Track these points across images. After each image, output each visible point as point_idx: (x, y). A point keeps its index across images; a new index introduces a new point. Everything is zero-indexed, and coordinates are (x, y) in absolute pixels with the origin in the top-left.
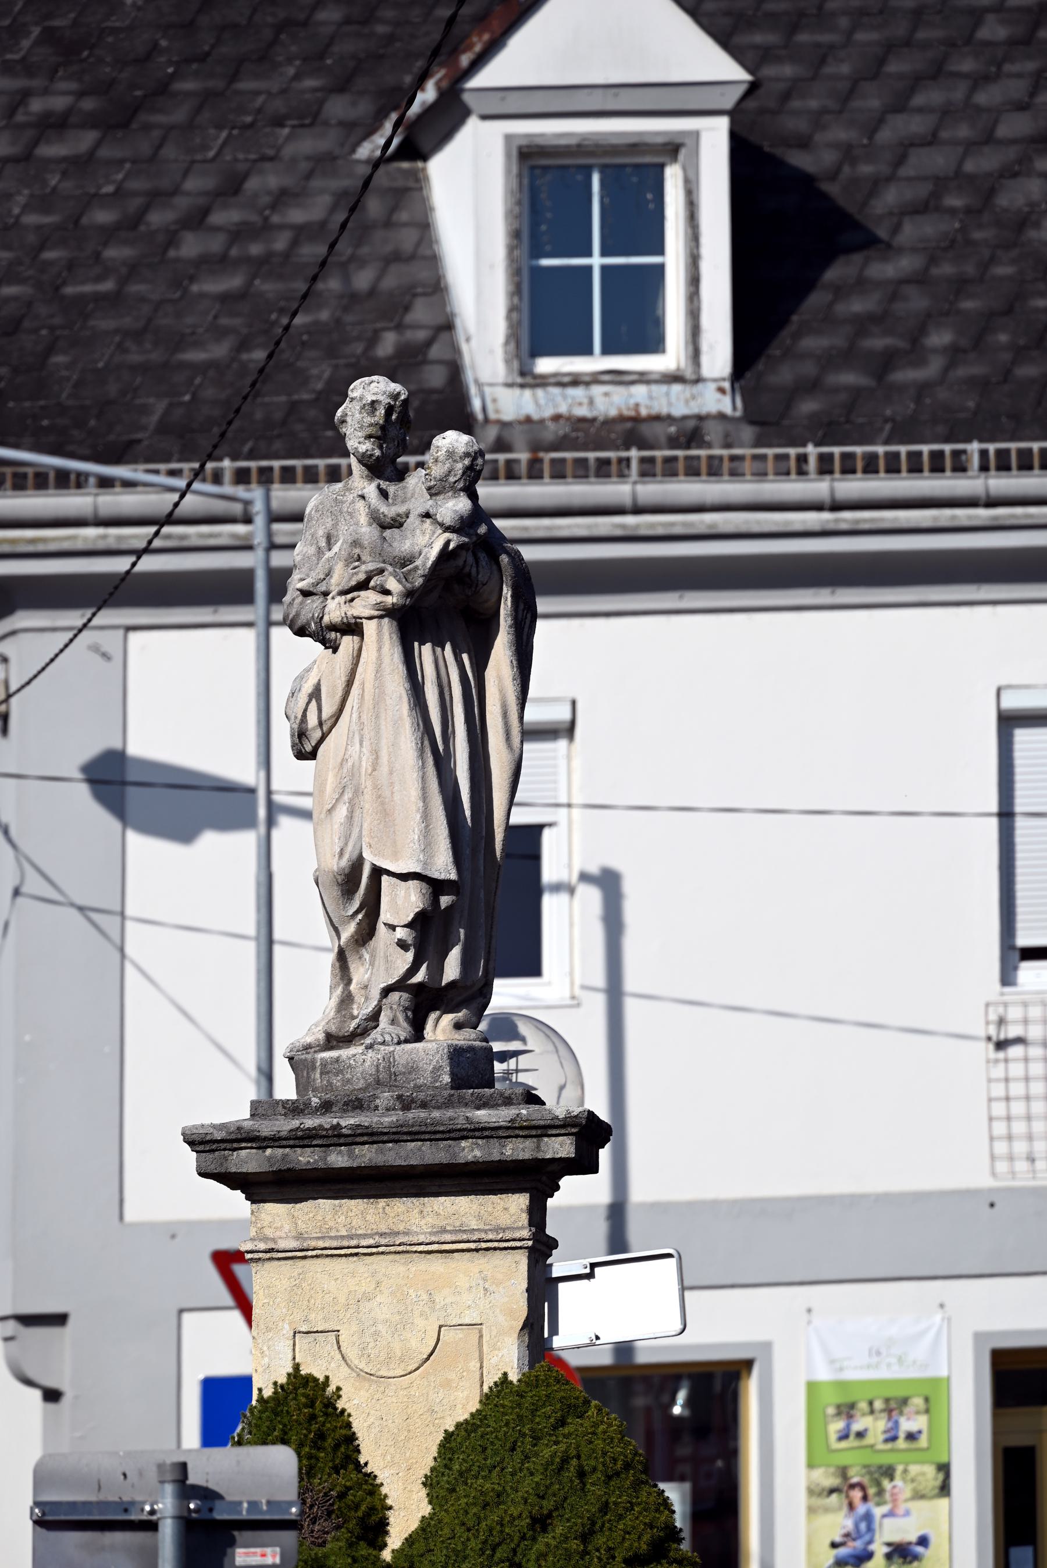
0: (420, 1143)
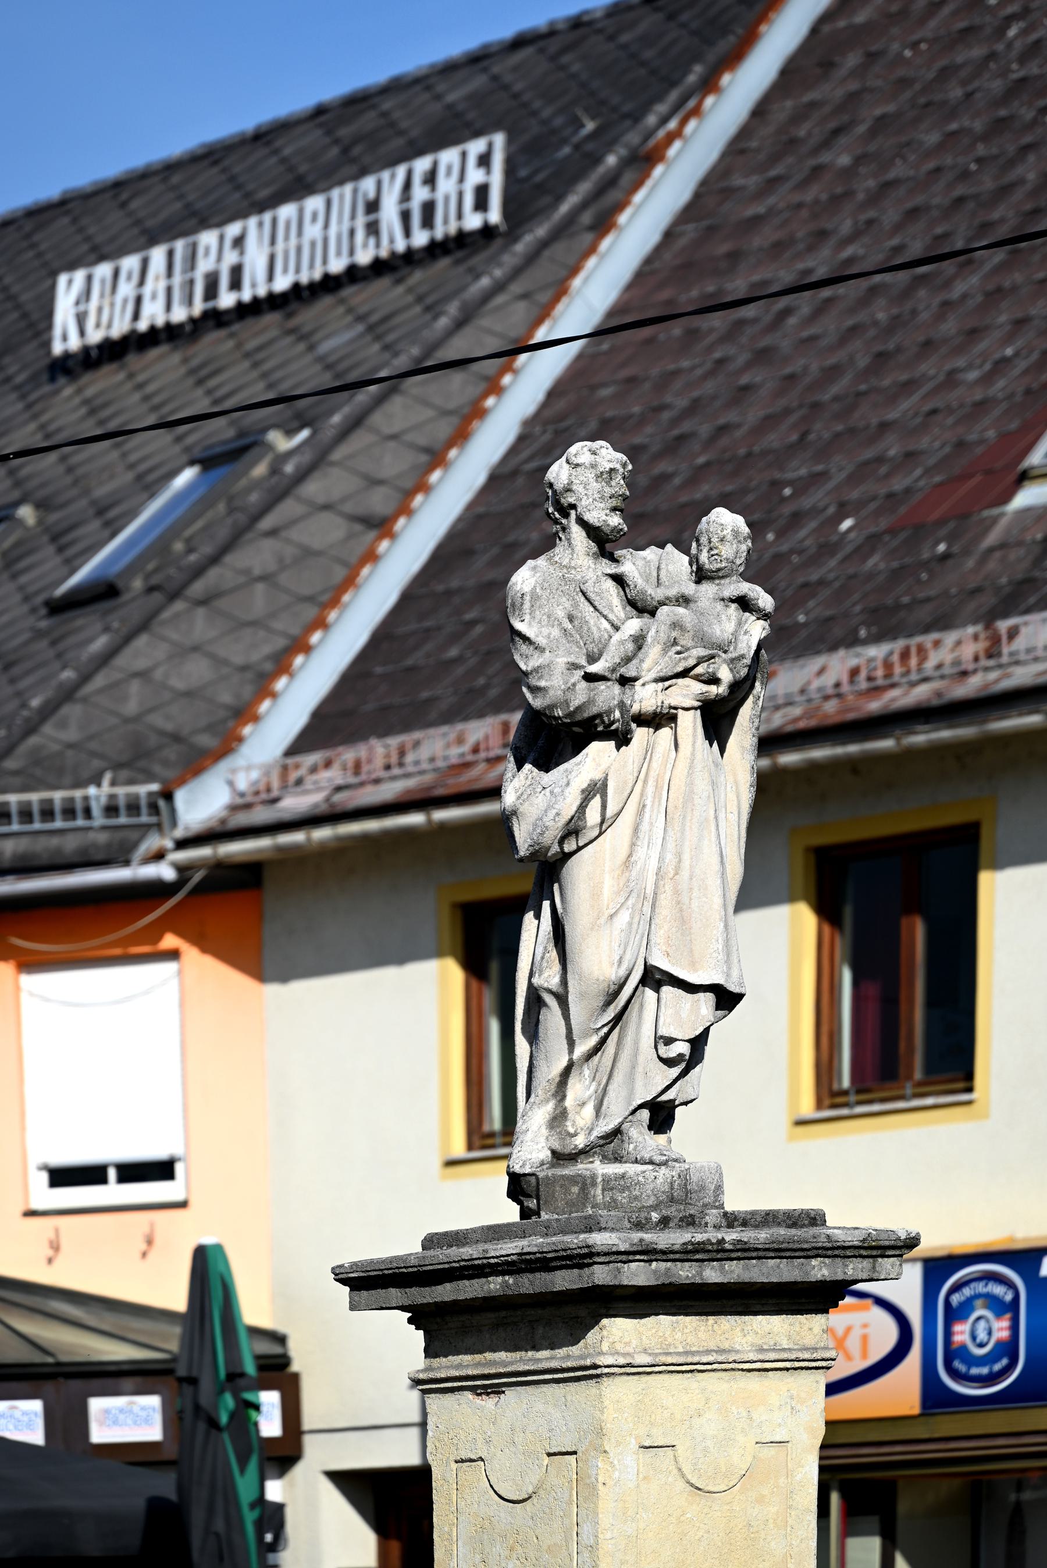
0: (778, 1260)
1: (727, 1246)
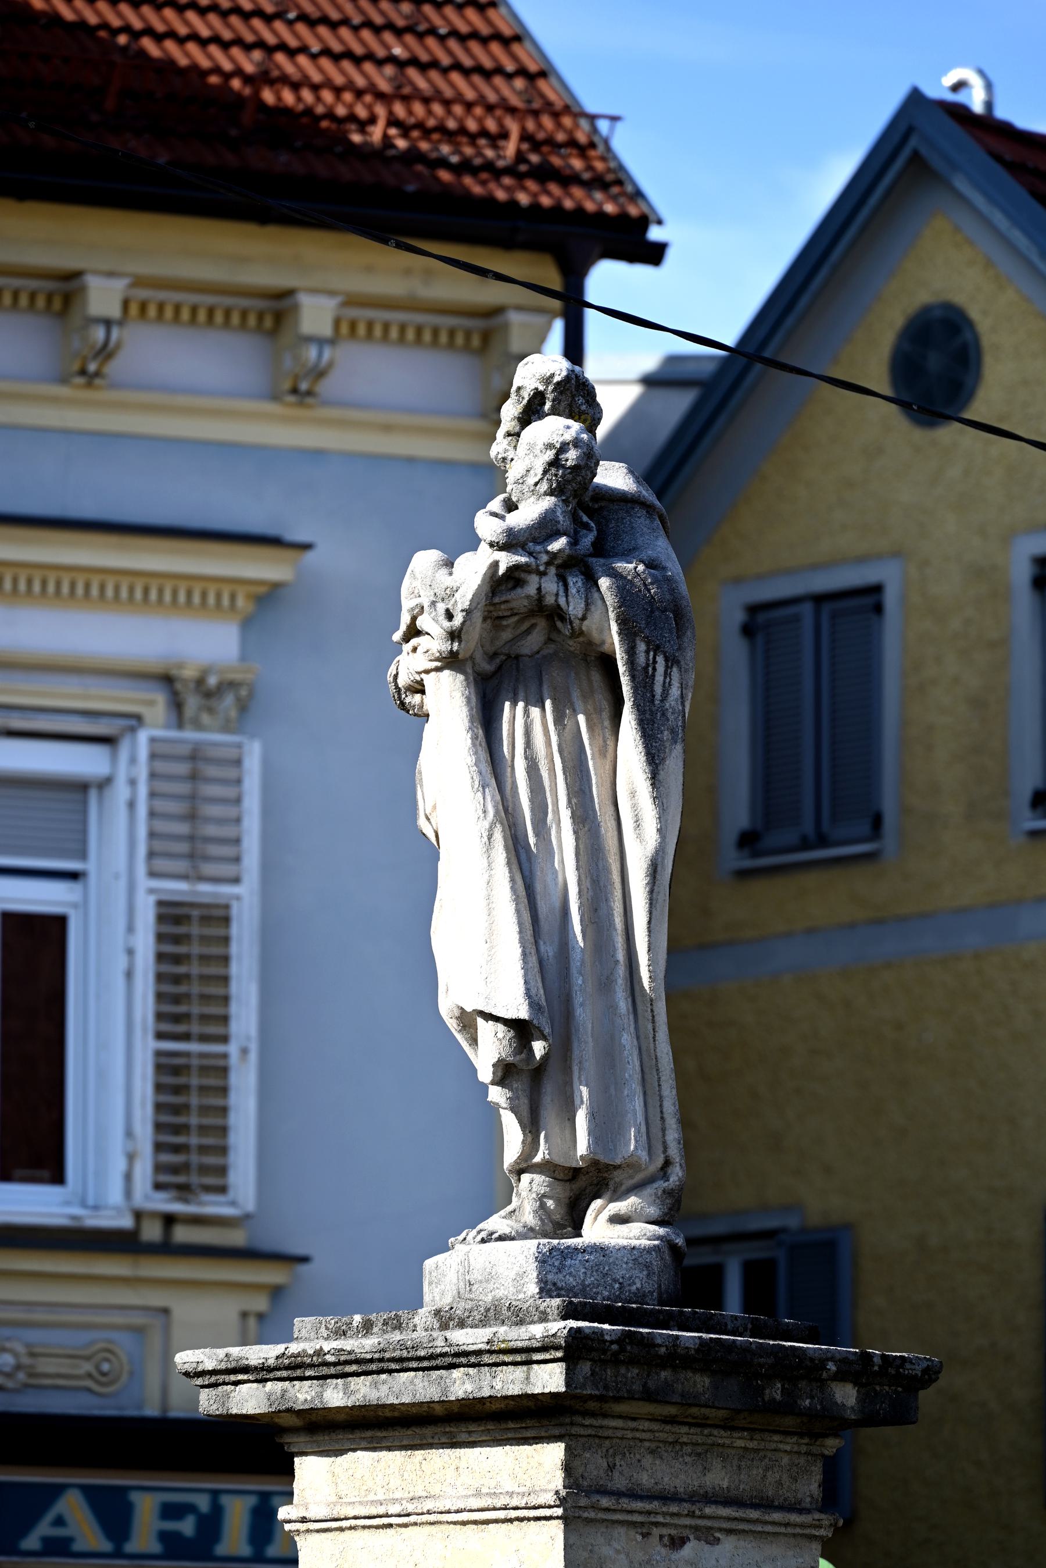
0: (412, 1374)
1: (330, 1358)
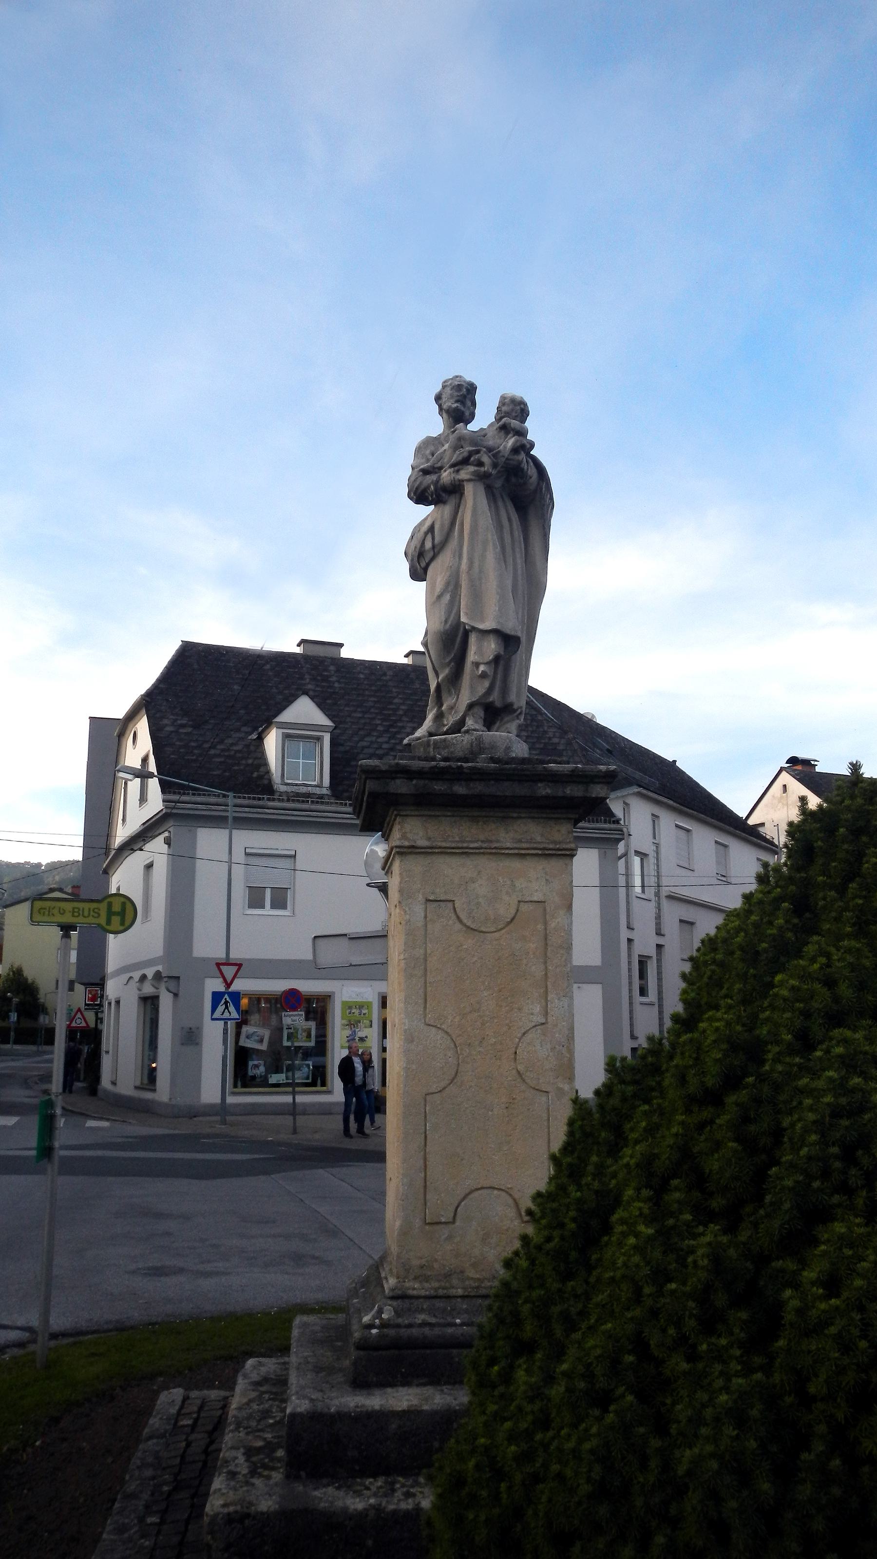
1: (465, 770)
